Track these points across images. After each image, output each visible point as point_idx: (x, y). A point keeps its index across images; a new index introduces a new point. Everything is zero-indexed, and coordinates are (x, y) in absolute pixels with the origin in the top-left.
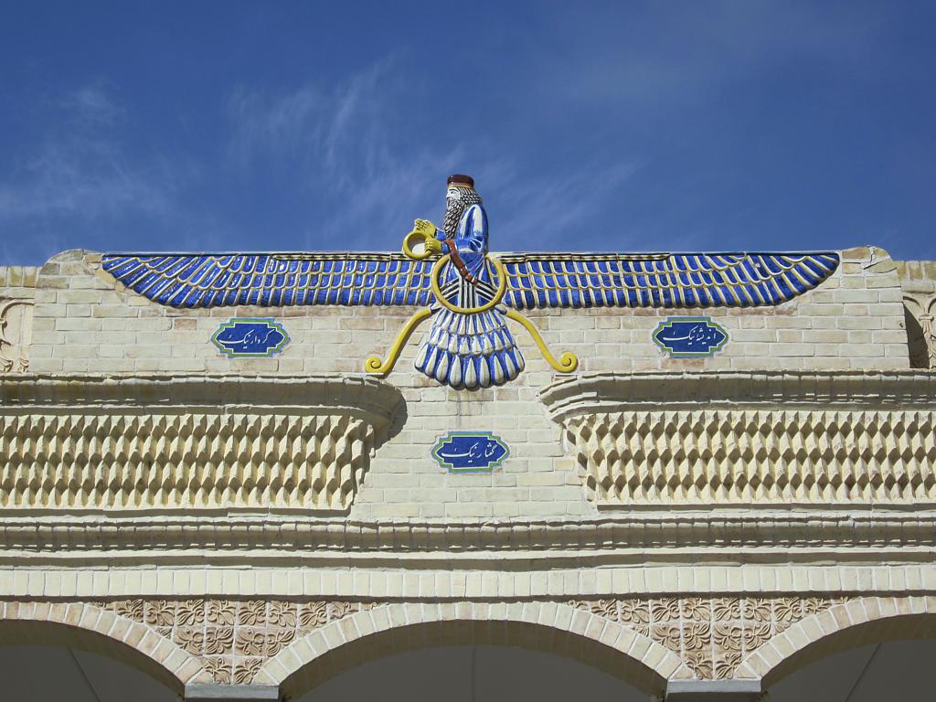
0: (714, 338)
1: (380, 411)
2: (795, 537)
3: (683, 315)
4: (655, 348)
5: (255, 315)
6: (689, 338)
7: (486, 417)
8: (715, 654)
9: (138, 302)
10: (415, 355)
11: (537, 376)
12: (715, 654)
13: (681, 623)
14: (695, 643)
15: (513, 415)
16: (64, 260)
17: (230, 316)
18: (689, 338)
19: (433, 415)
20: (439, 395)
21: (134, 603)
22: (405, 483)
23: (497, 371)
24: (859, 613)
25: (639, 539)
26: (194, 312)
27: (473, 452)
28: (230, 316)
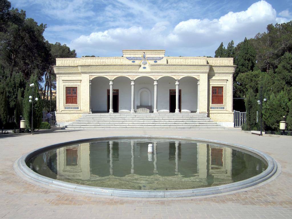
1: (140, 66)
2: (160, 72)
6: (156, 62)
7: (145, 66)
9: (128, 60)
10: (142, 63)
11: (148, 64)
14: (155, 77)
15: (146, 66)
17: (132, 60)
18: (156, 62)
19: (143, 66)
22: (141, 69)
25: (153, 72)
27: (145, 68)
28: (132, 60)
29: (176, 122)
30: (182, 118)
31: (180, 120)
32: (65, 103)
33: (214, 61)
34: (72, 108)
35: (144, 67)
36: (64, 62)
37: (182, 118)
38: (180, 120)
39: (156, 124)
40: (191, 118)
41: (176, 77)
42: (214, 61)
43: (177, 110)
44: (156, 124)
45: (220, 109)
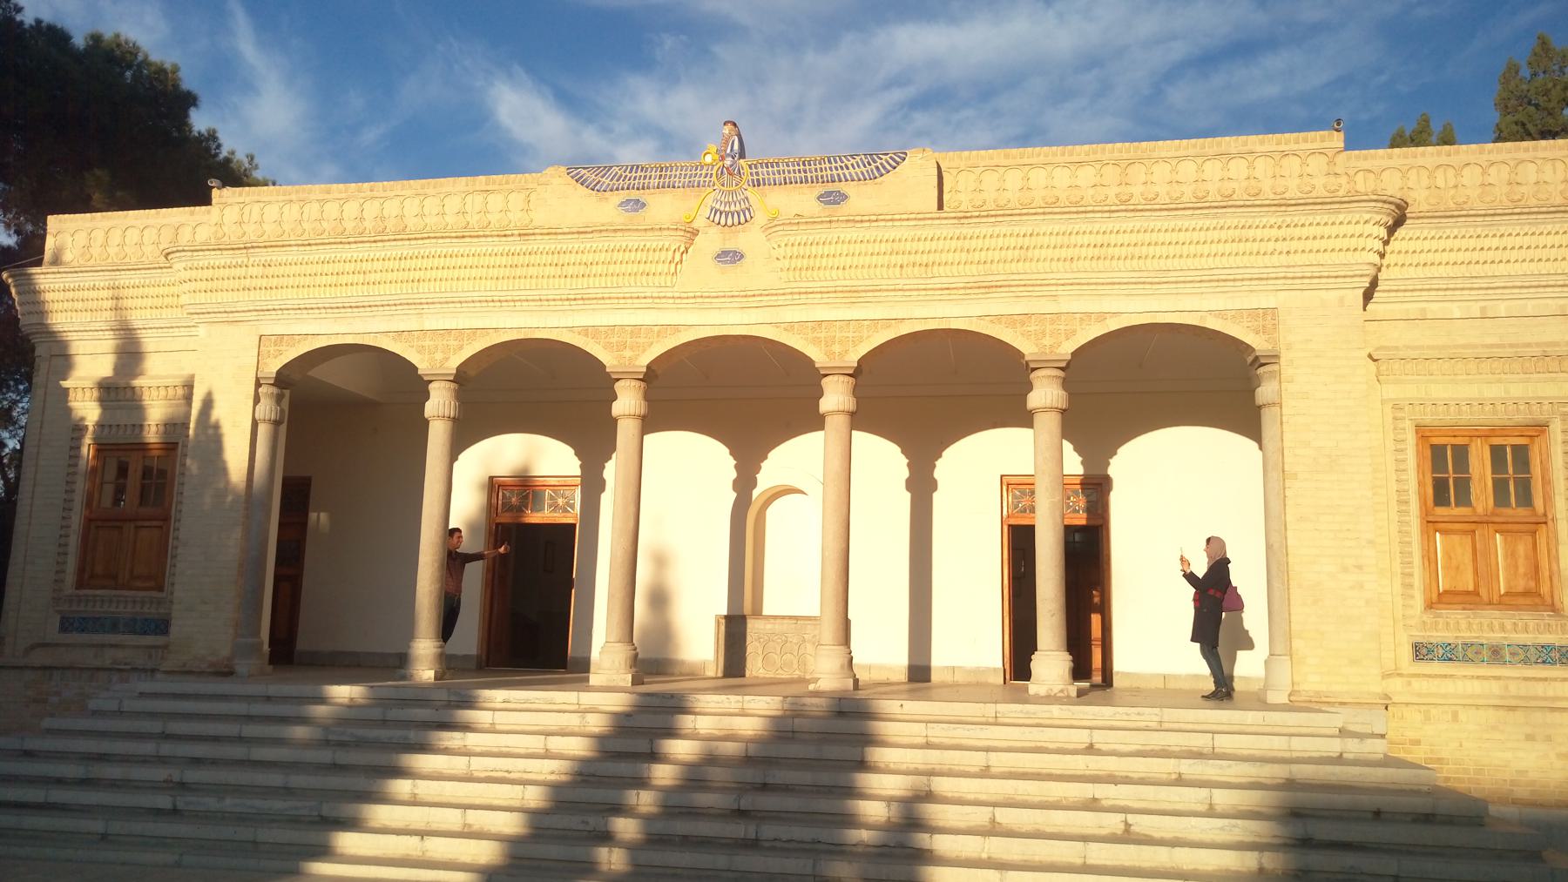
0: (844, 197)
3: (831, 187)
4: (816, 203)
5: (634, 194)
6: (833, 199)
8: (837, 348)
9: (582, 190)
11: (760, 218)
12: (837, 348)
13: (823, 335)
16: (550, 171)
17: (623, 195)
18: (833, 199)
20: (715, 230)
21: (585, 331)
22: (700, 269)
23: (743, 217)
24: (905, 329)
26: (608, 194)
27: (730, 257)
29: (1006, 817)
30: (1080, 764)
31: (1057, 790)
32: (70, 577)
33: (1425, 182)
34: (114, 627)
35: (725, 253)
36: (105, 245)
37: (1080, 764)
38: (1057, 790)
39: (769, 831)
40: (1189, 768)
41: (1026, 335)
42: (1425, 182)
43: (1051, 664)
44: (769, 831)
45: (1526, 661)
